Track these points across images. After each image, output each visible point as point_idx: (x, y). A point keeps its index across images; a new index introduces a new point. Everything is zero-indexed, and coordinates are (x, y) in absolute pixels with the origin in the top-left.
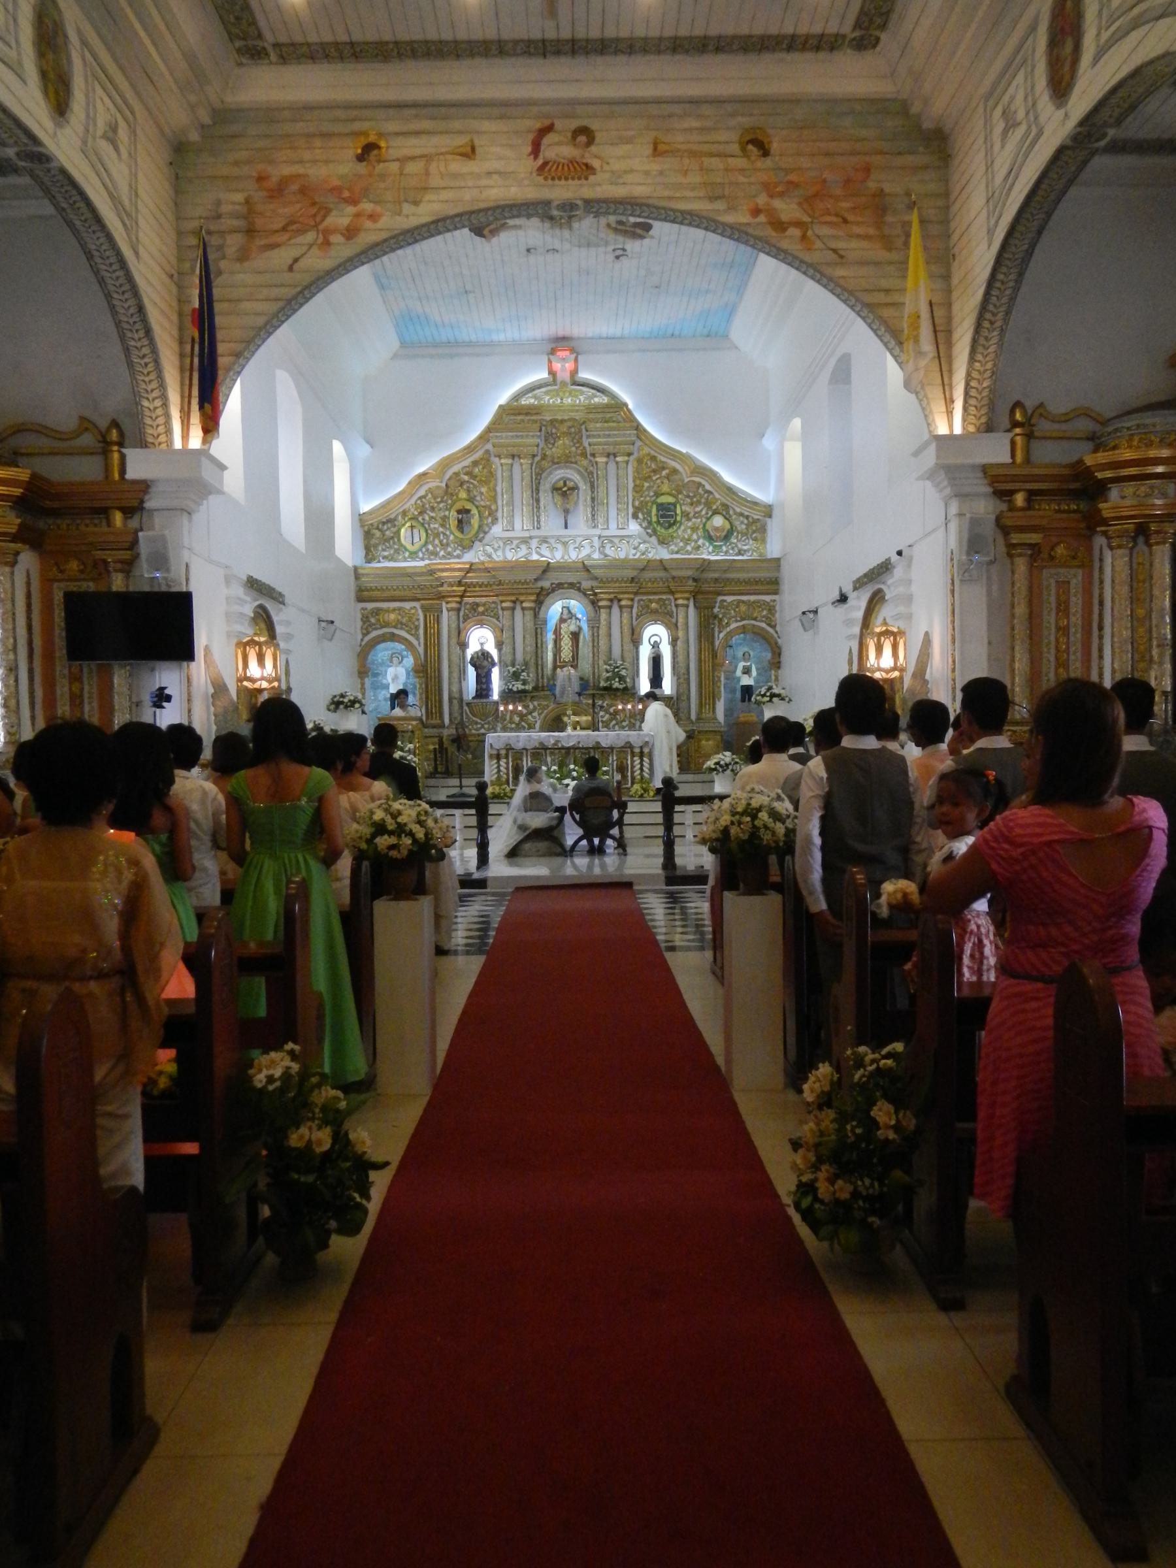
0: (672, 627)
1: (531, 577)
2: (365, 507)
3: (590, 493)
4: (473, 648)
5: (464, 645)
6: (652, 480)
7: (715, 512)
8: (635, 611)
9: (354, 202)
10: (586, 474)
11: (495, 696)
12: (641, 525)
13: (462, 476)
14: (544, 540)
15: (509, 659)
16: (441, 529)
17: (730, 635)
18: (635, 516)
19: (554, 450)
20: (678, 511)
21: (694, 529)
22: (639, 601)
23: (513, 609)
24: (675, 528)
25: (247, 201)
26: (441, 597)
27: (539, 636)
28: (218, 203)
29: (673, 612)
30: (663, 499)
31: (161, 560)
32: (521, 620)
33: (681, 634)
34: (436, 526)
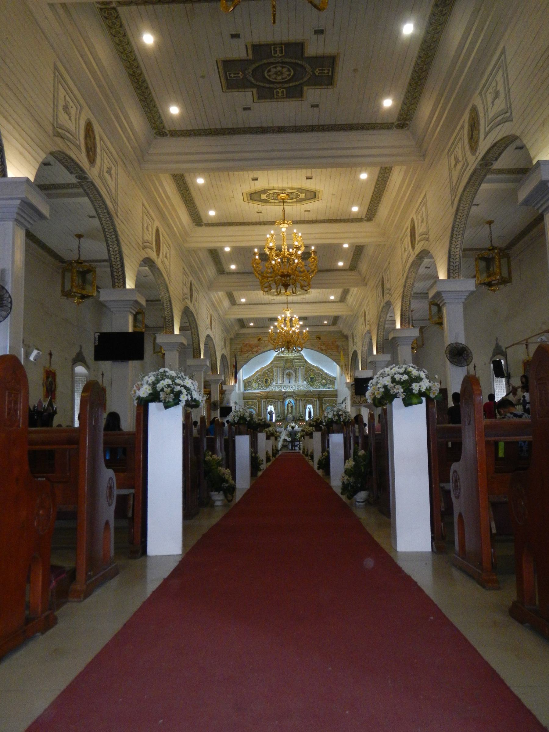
0: (313, 405)
1: (282, 394)
2: (245, 378)
4: (269, 410)
5: (267, 409)
7: (323, 379)
9: (257, 347)
11: (274, 421)
14: (285, 386)
15: (277, 412)
17: (327, 407)
18: (305, 380)
21: (318, 383)
23: (278, 401)
25: (241, 347)
26: (262, 399)
28: (237, 347)
30: (312, 376)
31: (228, 402)
32: (279, 404)
33: (315, 407)
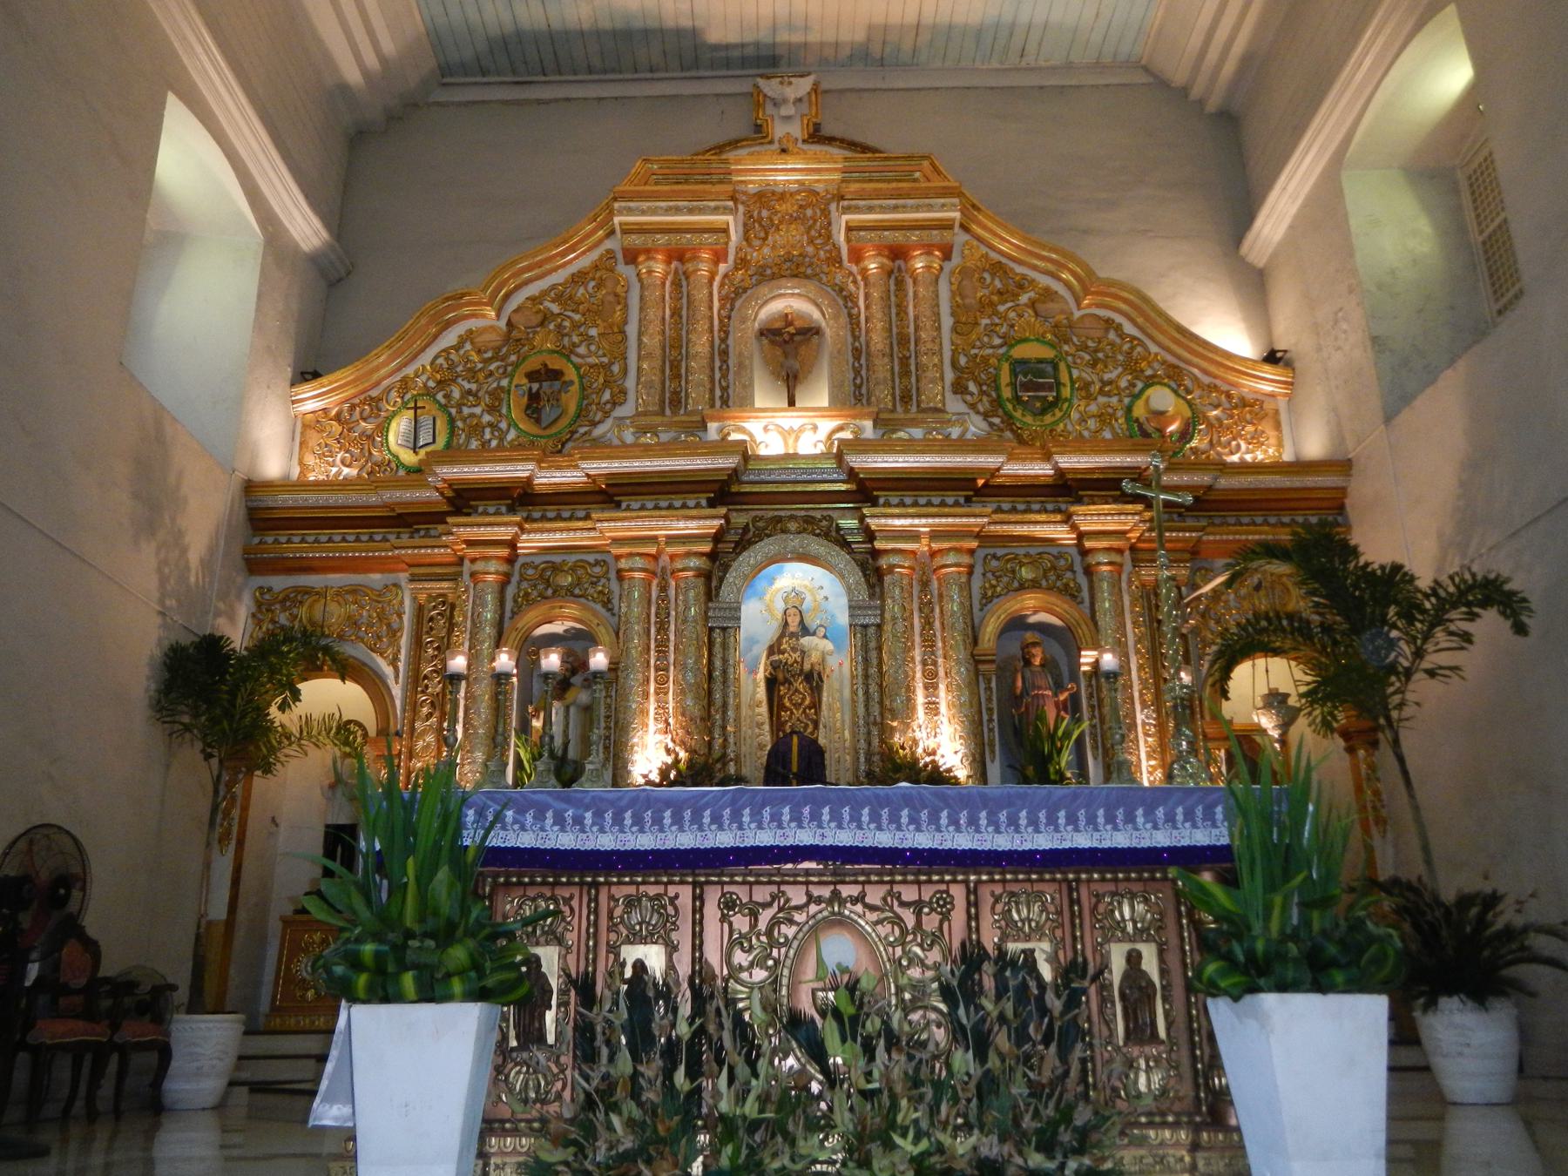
3: (850, 339)
6: (996, 313)
7: (1150, 382)
8: (977, 583)
10: (841, 302)
12: (973, 406)
13: (547, 304)
16: (487, 418)
18: (959, 388)
19: (766, 250)
20: (1064, 378)
22: (986, 557)
24: (1059, 414)
27: (717, 649)
29: (1079, 589)
30: (1020, 352)
34: (478, 410)
